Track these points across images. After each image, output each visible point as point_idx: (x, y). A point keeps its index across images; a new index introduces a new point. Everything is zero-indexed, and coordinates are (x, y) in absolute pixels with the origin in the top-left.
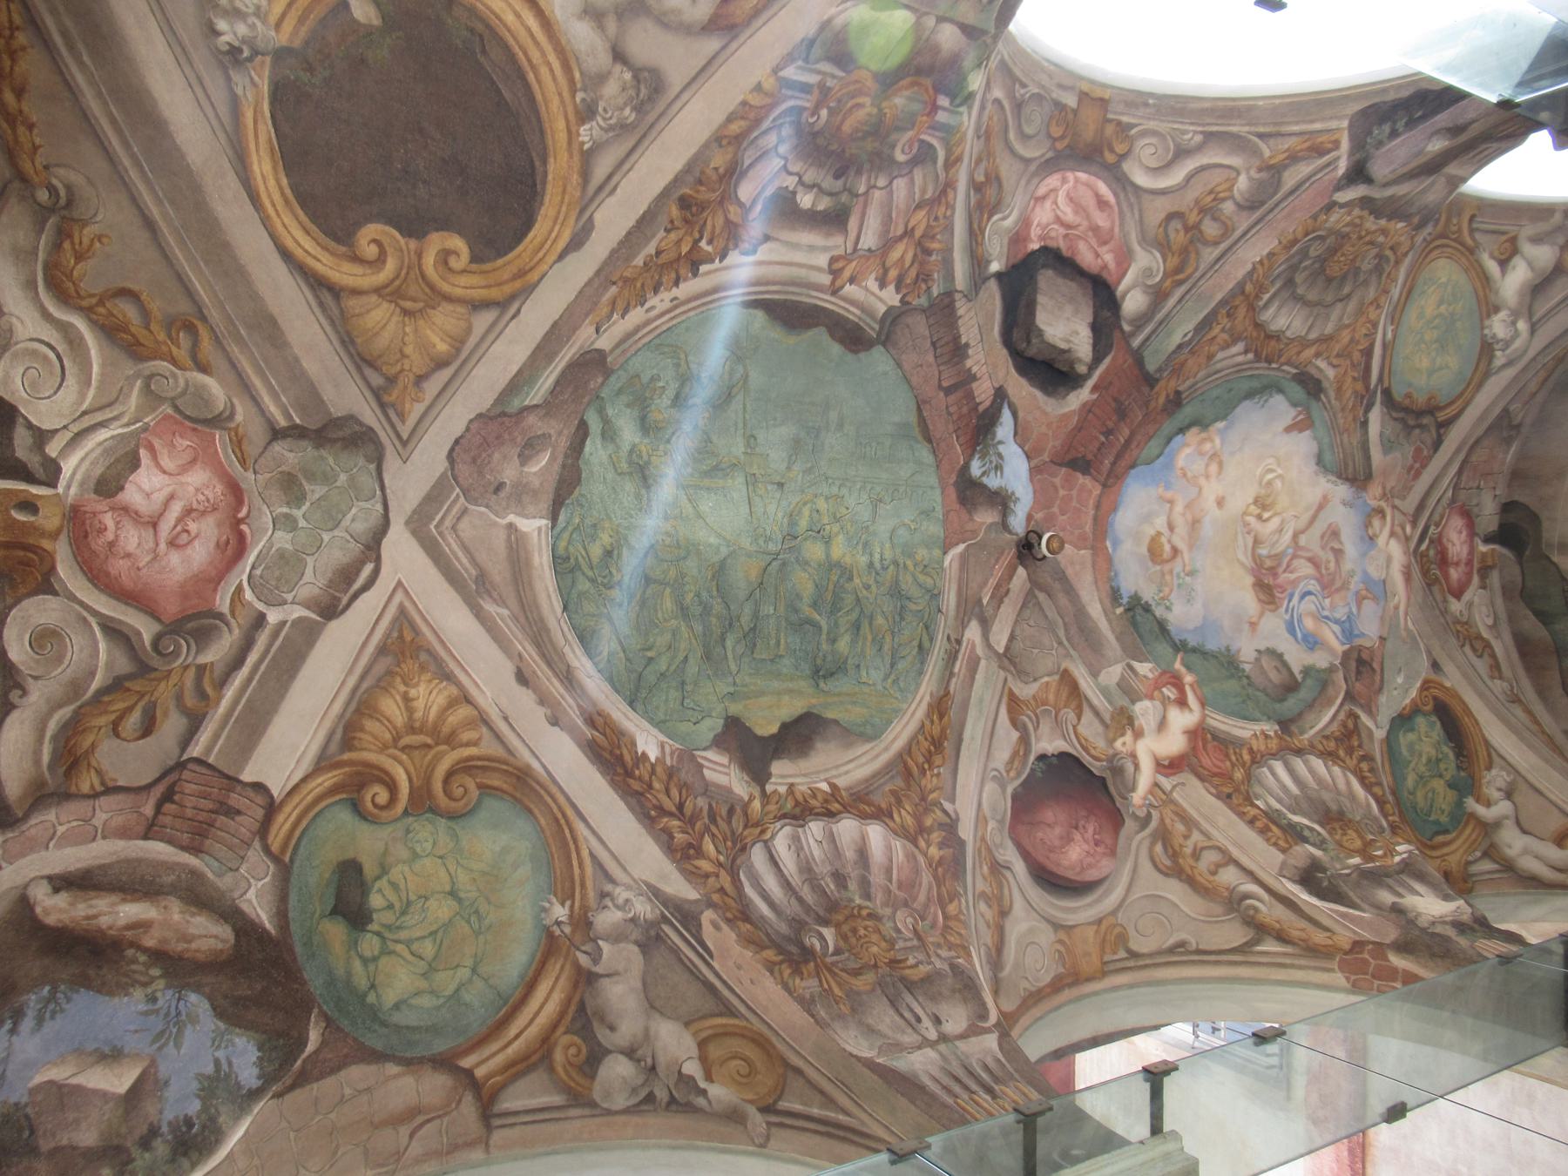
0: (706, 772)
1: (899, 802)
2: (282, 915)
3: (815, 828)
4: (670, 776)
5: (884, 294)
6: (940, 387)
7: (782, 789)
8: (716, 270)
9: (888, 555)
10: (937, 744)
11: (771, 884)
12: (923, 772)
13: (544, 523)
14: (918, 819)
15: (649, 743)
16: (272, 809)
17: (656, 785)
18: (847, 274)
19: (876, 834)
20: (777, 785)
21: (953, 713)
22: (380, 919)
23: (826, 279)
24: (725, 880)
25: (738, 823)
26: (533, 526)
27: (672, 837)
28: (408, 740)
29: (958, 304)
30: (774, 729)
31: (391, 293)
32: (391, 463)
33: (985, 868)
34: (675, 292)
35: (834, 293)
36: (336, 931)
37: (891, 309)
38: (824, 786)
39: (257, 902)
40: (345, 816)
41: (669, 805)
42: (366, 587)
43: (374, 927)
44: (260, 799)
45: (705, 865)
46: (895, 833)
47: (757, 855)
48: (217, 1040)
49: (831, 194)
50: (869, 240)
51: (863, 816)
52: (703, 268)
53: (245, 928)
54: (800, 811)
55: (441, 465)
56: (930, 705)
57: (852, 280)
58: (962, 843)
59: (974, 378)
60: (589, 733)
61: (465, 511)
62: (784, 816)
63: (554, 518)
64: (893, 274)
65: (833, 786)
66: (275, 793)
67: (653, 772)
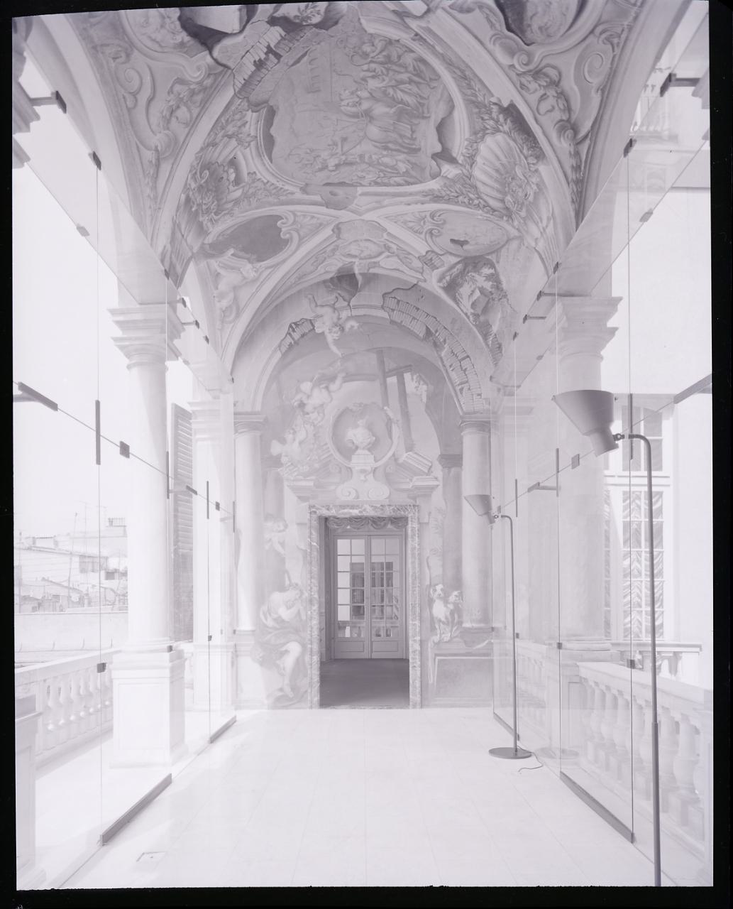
0: (449, 176)
1: (482, 119)
2: (458, 256)
3: (479, 159)
4: (447, 188)
5: (249, 120)
6: (279, 62)
7: (462, 158)
8: (264, 177)
9: (365, 67)
10: (465, 78)
11: (488, 190)
12: (476, 96)
13: (358, 188)
14: (493, 119)
15: (434, 185)
16: (433, 252)
17: (448, 192)
18: (248, 139)
19: (489, 139)
20: (460, 159)
21: (454, 59)
22: (467, 239)
23: (253, 144)
24: (481, 201)
25: (468, 181)
26: (360, 190)
27: (465, 203)
28: (422, 223)
29: (240, 86)
30: (440, 145)
31: (297, 231)
32: (341, 221)
33: (533, 86)
34: (275, 182)
35: (256, 137)
36: (466, 247)
37: (253, 111)
38: (466, 143)
39: (454, 260)
40: (438, 239)
41: (456, 195)
42: (379, 224)
43: (469, 240)
44: (430, 253)
45: (476, 202)
46: (493, 134)
47: (479, 185)
48: (480, 275)
49: (227, 173)
50: (234, 142)
51: (483, 138)
52: (265, 181)
53: (459, 262)
54: (471, 159)
55: (343, 211)
56: (446, 68)
57: (249, 135)
58: (511, 112)
59: (269, 47)
60: (427, 199)
61: (356, 205)
62: (471, 166)
63: (357, 186)
64: (239, 124)
65: (466, 140)
66: (429, 249)
67: (445, 191)
